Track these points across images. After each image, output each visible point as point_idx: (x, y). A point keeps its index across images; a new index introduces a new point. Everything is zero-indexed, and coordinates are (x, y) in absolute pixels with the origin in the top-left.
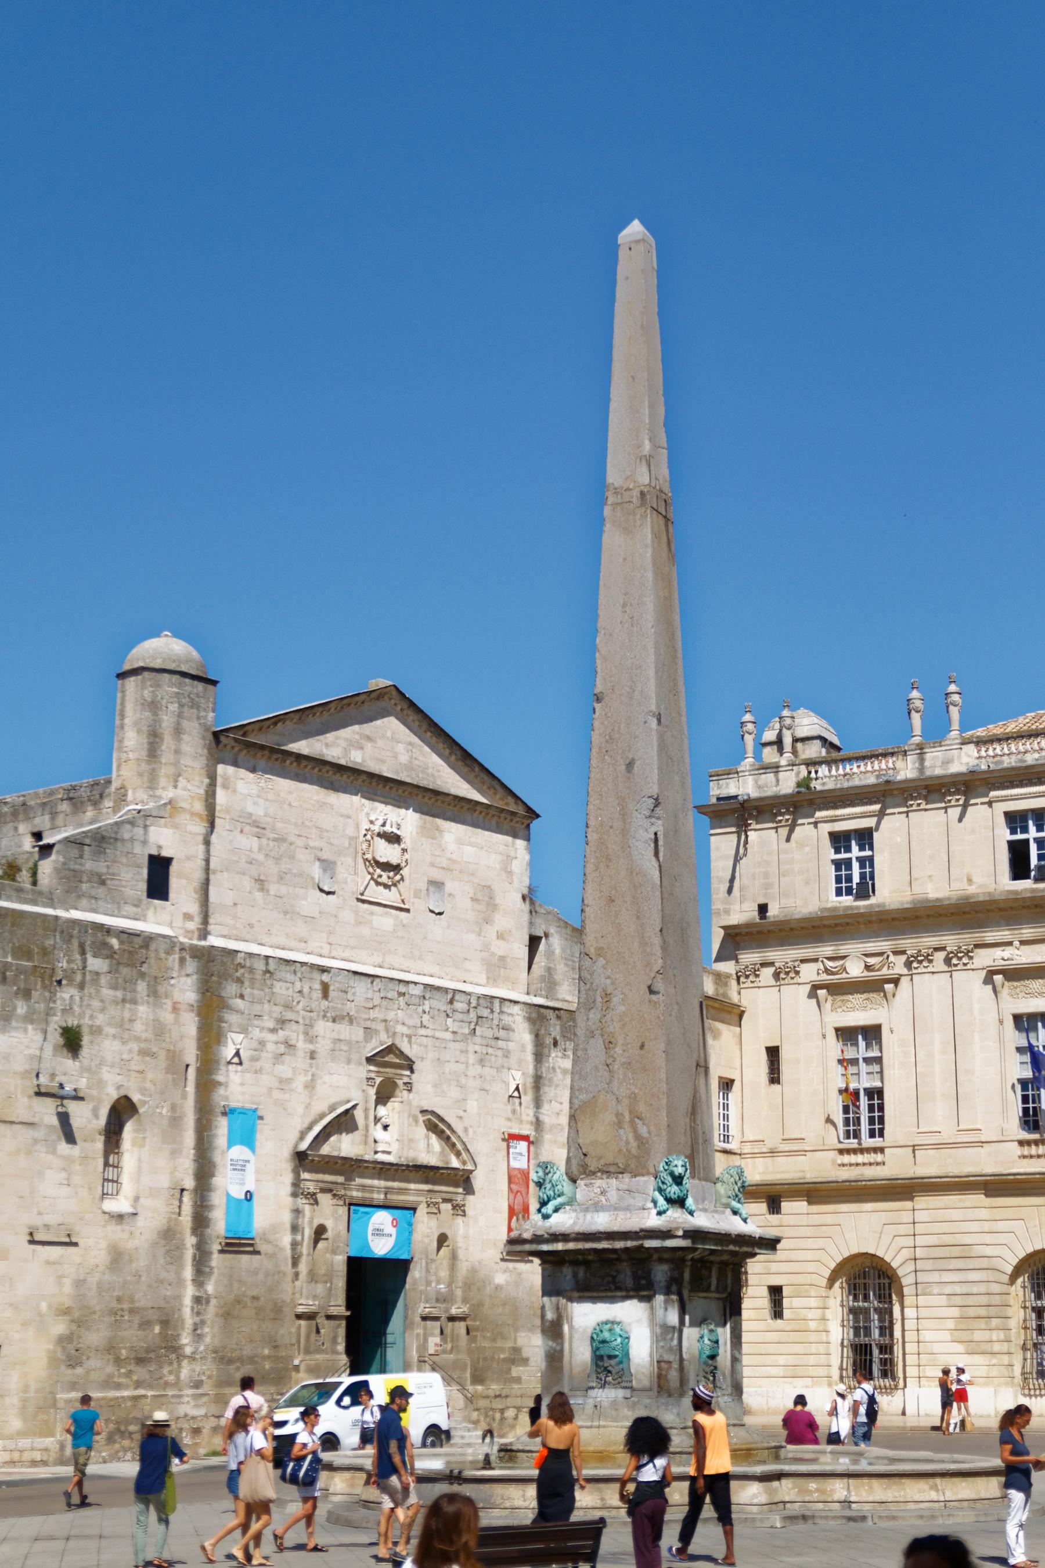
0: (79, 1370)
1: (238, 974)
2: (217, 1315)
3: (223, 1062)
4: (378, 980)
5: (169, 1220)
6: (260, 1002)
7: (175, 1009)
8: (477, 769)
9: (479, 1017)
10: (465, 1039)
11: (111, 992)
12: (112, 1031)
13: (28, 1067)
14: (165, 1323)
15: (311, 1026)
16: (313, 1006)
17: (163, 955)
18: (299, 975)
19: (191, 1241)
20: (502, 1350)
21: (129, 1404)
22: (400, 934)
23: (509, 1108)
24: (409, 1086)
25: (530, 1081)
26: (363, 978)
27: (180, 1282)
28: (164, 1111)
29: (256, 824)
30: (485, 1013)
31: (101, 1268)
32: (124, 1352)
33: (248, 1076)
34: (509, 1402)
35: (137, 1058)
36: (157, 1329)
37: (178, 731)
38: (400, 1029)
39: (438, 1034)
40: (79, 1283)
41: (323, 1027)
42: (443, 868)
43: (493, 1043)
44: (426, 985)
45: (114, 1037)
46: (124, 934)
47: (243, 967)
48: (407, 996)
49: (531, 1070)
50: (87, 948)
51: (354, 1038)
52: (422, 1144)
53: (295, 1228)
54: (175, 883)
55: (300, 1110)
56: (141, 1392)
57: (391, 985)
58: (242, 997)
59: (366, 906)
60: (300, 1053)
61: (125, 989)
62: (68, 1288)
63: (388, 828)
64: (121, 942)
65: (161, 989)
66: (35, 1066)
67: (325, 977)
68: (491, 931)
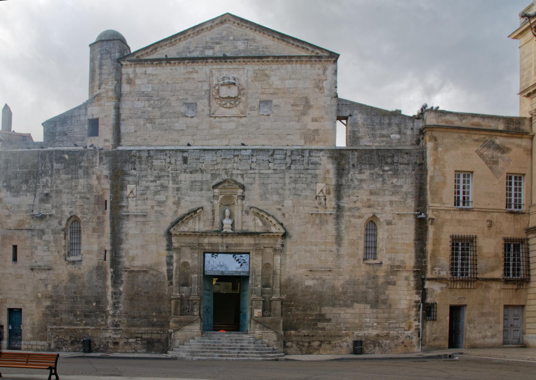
0: (57, 318)
1: (133, 160)
2: (126, 299)
3: (125, 197)
5: (99, 263)
6: (146, 170)
7: (98, 178)
8: (292, 42)
10: (283, 172)
11: (66, 176)
12: (67, 191)
13: (28, 209)
14: (98, 302)
16: (178, 168)
17: (91, 158)
18: (168, 155)
19: (110, 271)
20: (310, 315)
21: (81, 331)
22: (240, 129)
23: (317, 202)
24: (243, 197)
25: (332, 189)
27: (106, 287)
28: (94, 220)
29: (147, 95)
30: (298, 158)
31: (66, 281)
32: (78, 312)
33: (139, 202)
34: (314, 338)
35: (79, 200)
36: (94, 304)
38: (235, 172)
39: (265, 172)
40: (55, 287)
41: (182, 177)
42: (271, 94)
43: (304, 172)
44: (253, 150)
45: (68, 193)
46: (68, 152)
48: (240, 156)
50: (54, 160)
51: (204, 179)
52: (251, 224)
53: (169, 264)
54: (101, 128)
55: (171, 213)
56: (88, 327)
57: (228, 153)
58: (135, 169)
59: (217, 119)
60: (170, 190)
61: (72, 174)
62: (50, 288)
63: (226, 81)
64: (69, 156)
65: (90, 172)
66: (31, 208)
67: (185, 154)
68: (307, 119)
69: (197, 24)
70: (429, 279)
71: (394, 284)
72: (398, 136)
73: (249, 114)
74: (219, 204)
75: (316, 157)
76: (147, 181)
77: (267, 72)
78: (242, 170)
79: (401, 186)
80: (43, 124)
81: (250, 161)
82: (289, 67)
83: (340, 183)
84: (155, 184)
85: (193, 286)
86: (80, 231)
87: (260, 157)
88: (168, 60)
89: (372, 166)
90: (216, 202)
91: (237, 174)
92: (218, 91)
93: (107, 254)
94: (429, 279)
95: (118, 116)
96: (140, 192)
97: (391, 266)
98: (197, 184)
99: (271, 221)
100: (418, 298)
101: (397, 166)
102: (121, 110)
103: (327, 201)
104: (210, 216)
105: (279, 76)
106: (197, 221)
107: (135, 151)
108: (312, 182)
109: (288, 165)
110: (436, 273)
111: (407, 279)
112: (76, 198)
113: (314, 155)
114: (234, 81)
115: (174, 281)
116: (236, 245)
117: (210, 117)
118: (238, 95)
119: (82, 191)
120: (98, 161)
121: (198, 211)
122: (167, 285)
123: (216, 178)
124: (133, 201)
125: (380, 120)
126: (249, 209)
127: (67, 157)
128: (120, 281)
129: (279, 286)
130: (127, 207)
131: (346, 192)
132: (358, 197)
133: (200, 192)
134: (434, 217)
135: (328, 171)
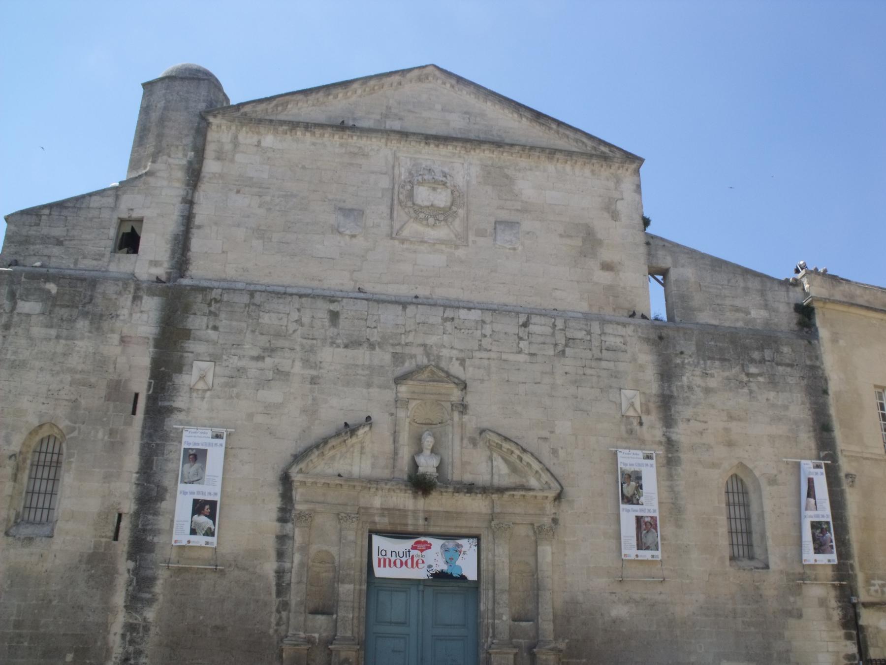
1: (212, 309)
4: (411, 310)
5: (97, 546)
7: (123, 340)
8: (554, 126)
9: (568, 339)
12: (37, 364)
15: (312, 350)
19: (124, 566)
23: (623, 428)
24: (463, 408)
26: (390, 306)
27: (108, 609)
37: (162, 121)
38: (445, 352)
39: (511, 357)
41: (328, 355)
42: (517, 210)
43: (594, 364)
45: (41, 369)
47: (216, 301)
48: (456, 321)
49: (654, 388)
58: (215, 328)
65: (106, 325)
67: (334, 307)
69: (373, 74)
70: (866, 605)
71: (800, 616)
72: (763, 314)
73: (474, 242)
74: (408, 420)
75: (615, 336)
76: (240, 358)
77: (510, 172)
78: (461, 351)
79: (786, 408)
80: (7, 218)
81: (479, 332)
82: (551, 167)
83: (667, 392)
84: (260, 364)
85: (341, 613)
86: (58, 462)
87: (498, 327)
88: (308, 126)
89: (727, 363)
90: (401, 414)
91: (451, 358)
92: (411, 195)
93: (122, 524)
94: (866, 605)
95: (188, 221)
96: (223, 380)
97: (788, 574)
98: (360, 372)
99: (529, 465)
100: (852, 649)
101: (772, 367)
102: (195, 206)
103: (645, 427)
104: (389, 447)
105: (535, 181)
106: (357, 454)
107: (220, 291)
108: (611, 387)
109: (560, 348)
110: (876, 591)
111: (822, 602)
112: (61, 382)
113: (611, 331)
114: (444, 179)
115: (294, 598)
116: (448, 515)
117: (392, 238)
118: (452, 204)
119: (80, 368)
120: (129, 303)
121: (361, 432)
122: (274, 609)
123: (403, 363)
124: (203, 398)
125: (729, 281)
126: (477, 436)
127: (52, 287)
128: (148, 596)
129: (551, 617)
130: (188, 411)
131: (683, 411)
132: (706, 422)
133: (365, 391)
134: (853, 472)
135: (641, 368)
